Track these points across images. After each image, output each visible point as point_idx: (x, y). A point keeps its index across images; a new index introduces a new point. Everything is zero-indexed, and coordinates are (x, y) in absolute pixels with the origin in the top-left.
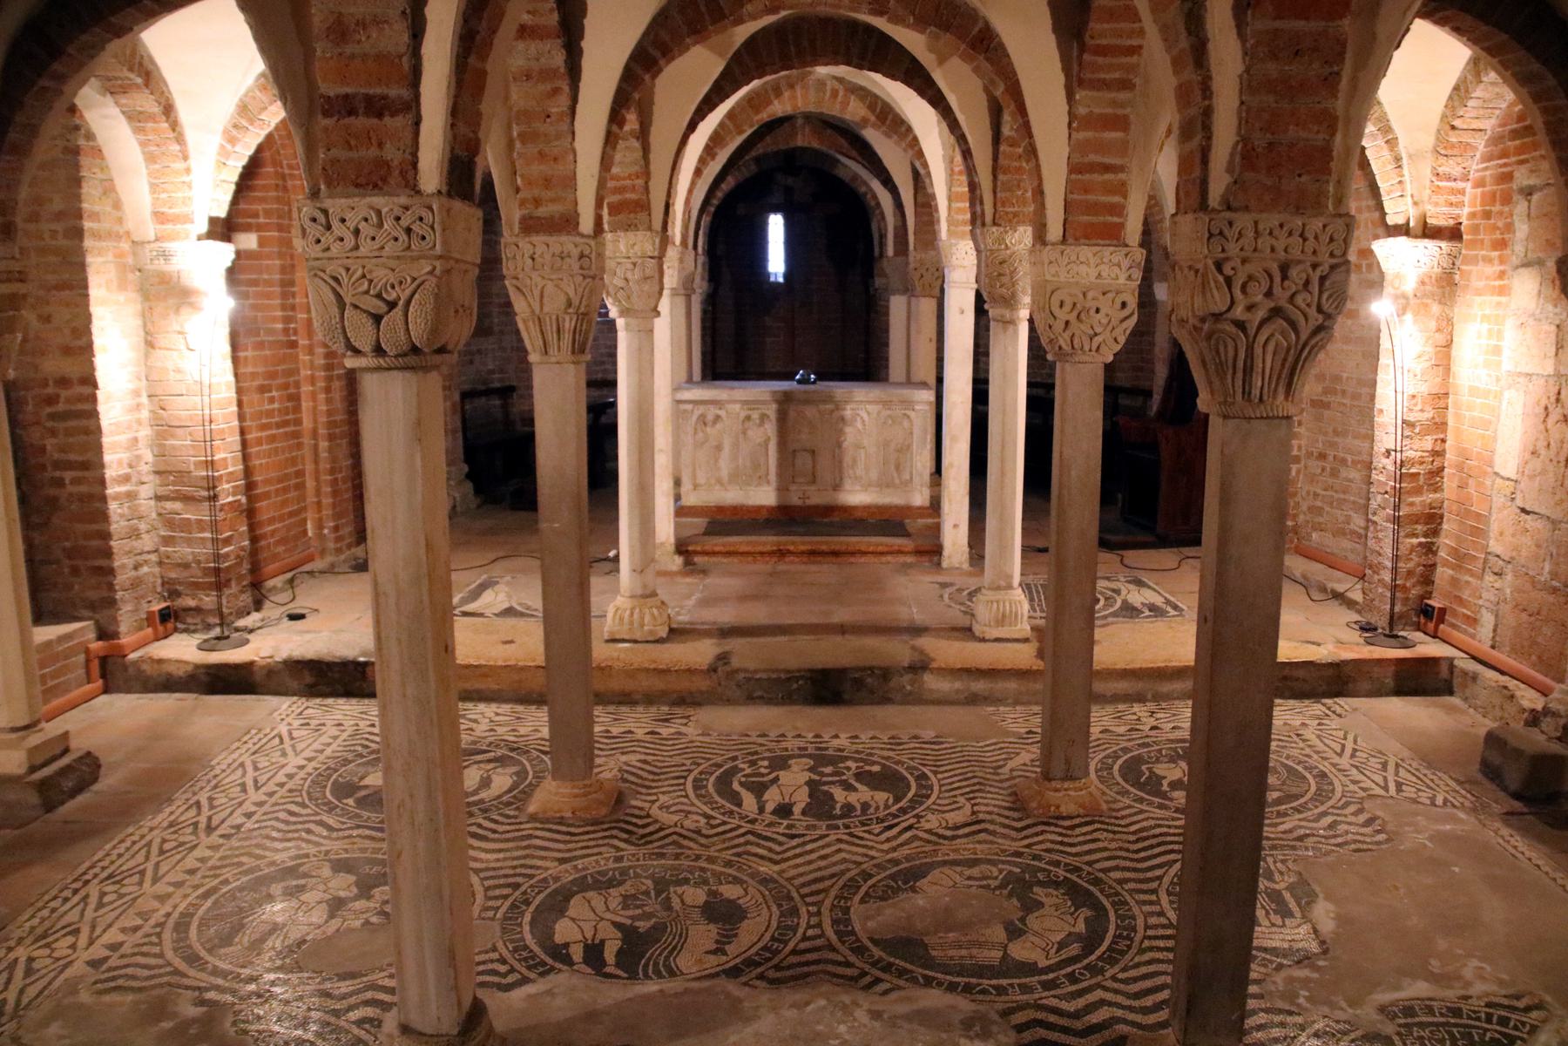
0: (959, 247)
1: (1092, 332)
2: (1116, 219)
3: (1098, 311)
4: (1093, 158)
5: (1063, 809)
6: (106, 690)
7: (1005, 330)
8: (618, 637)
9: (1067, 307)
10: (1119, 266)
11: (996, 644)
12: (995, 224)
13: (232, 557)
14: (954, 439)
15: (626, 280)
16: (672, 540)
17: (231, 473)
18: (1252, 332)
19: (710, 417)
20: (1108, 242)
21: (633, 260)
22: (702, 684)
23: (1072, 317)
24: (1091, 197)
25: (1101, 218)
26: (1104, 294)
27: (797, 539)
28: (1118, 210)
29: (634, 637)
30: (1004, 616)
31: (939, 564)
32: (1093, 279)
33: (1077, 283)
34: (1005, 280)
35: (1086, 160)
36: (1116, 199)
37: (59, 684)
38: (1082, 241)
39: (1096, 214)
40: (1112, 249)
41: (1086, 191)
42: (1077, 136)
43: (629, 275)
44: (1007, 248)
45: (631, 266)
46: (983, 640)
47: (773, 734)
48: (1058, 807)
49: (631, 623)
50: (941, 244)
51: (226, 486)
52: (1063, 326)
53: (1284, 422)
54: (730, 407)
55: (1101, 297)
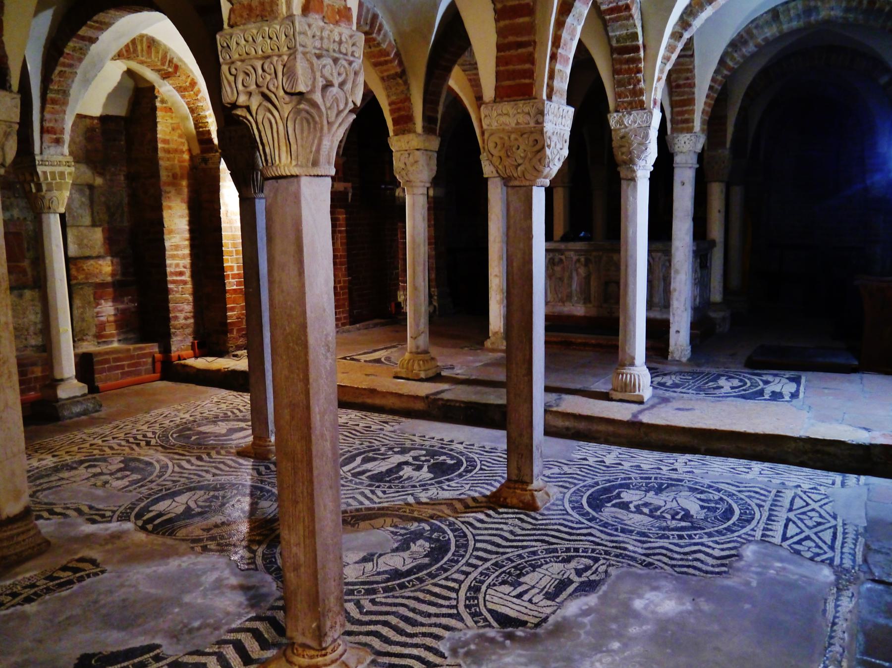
0: (679, 139)
1: (516, 163)
2: (527, 81)
3: (518, 148)
4: (511, 39)
5: (509, 500)
6: (162, 379)
7: (628, 185)
8: (399, 375)
9: (499, 147)
10: (529, 114)
11: (619, 404)
12: (617, 111)
13: (235, 318)
14: (677, 272)
15: (405, 164)
16: (502, 330)
17: (235, 274)
18: (254, 115)
19: (556, 260)
20: (521, 98)
21: (408, 152)
22: (420, 406)
23: (502, 154)
24: (511, 67)
25: (518, 81)
26: (522, 135)
27: (578, 335)
28: (530, 74)
29: (407, 376)
30: (626, 383)
31: (667, 358)
32: (513, 125)
33: (503, 130)
34: (624, 150)
35: (506, 41)
36: (527, 66)
37: (136, 370)
38: (505, 99)
39: (514, 79)
40: (523, 102)
41: (507, 64)
42: (502, 23)
43: (406, 161)
44: (626, 127)
45: (407, 156)
46: (611, 400)
47: (446, 439)
48: (505, 499)
49: (407, 369)
50: (666, 137)
51: (231, 280)
52: (499, 160)
53: (295, 180)
54: (567, 253)
55: (520, 140)
